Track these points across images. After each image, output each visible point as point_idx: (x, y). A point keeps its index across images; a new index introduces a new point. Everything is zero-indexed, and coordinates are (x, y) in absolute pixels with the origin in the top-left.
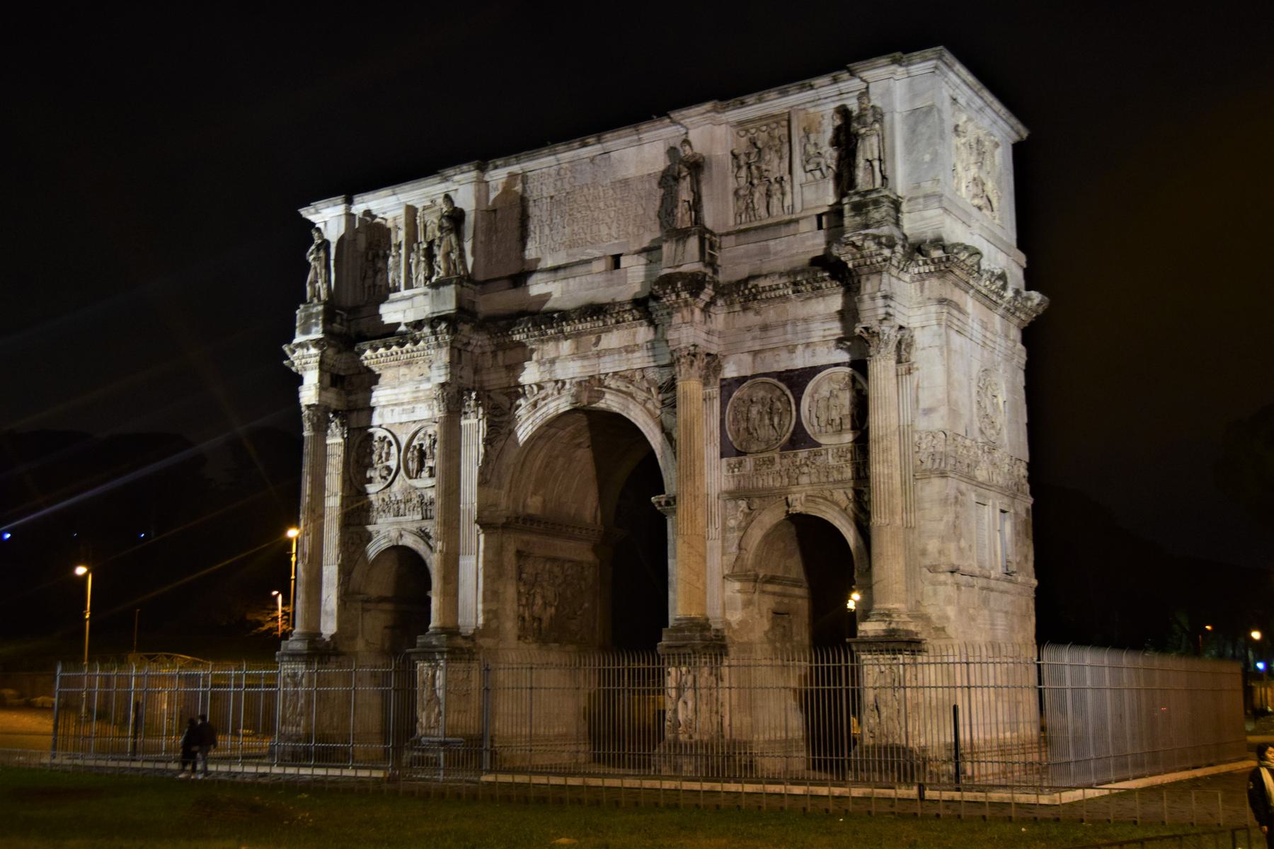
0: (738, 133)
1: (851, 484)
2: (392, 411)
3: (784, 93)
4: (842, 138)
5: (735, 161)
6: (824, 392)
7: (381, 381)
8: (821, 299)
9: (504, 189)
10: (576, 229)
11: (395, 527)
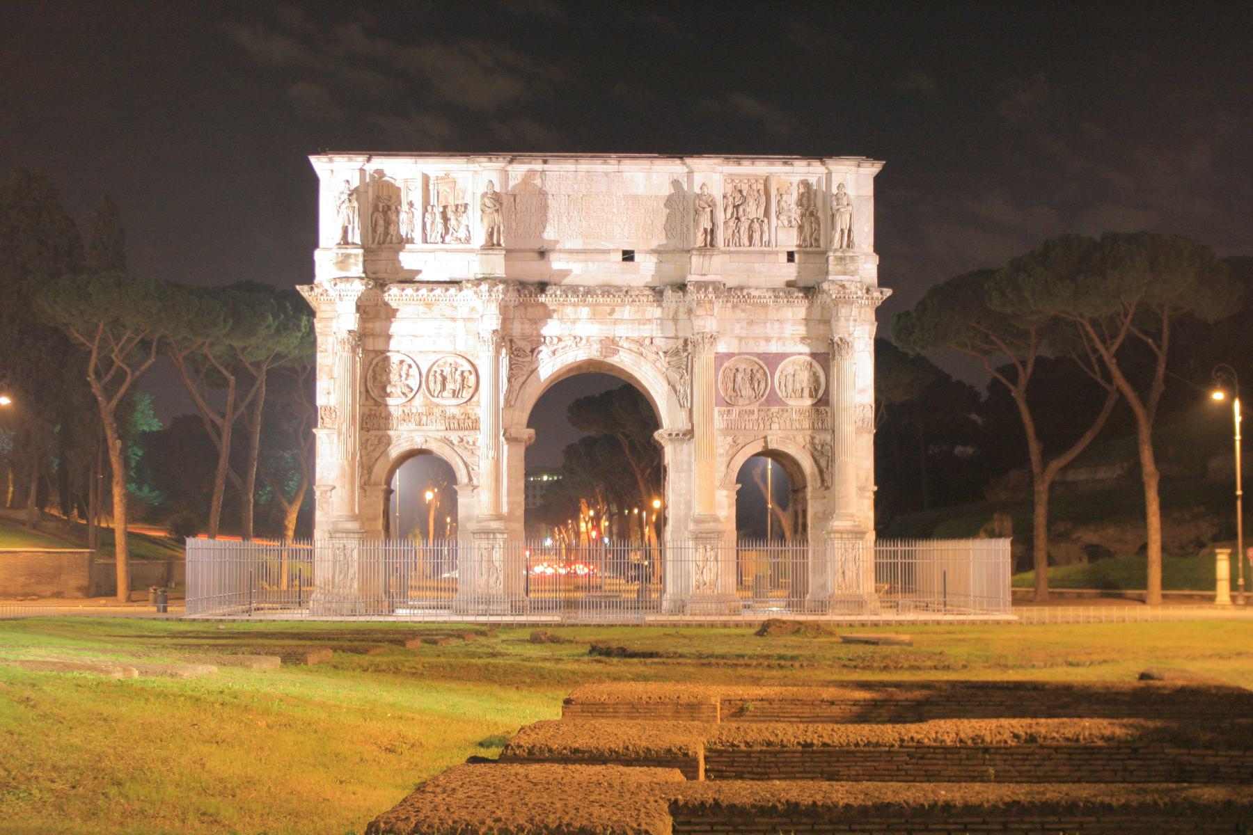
0: (725, 180)
1: (809, 432)
3: (772, 165)
4: (805, 201)
6: (790, 370)
7: (399, 315)
8: (790, 309)
9: (523, 180)
10: (592, 224)
11: (419, 434)
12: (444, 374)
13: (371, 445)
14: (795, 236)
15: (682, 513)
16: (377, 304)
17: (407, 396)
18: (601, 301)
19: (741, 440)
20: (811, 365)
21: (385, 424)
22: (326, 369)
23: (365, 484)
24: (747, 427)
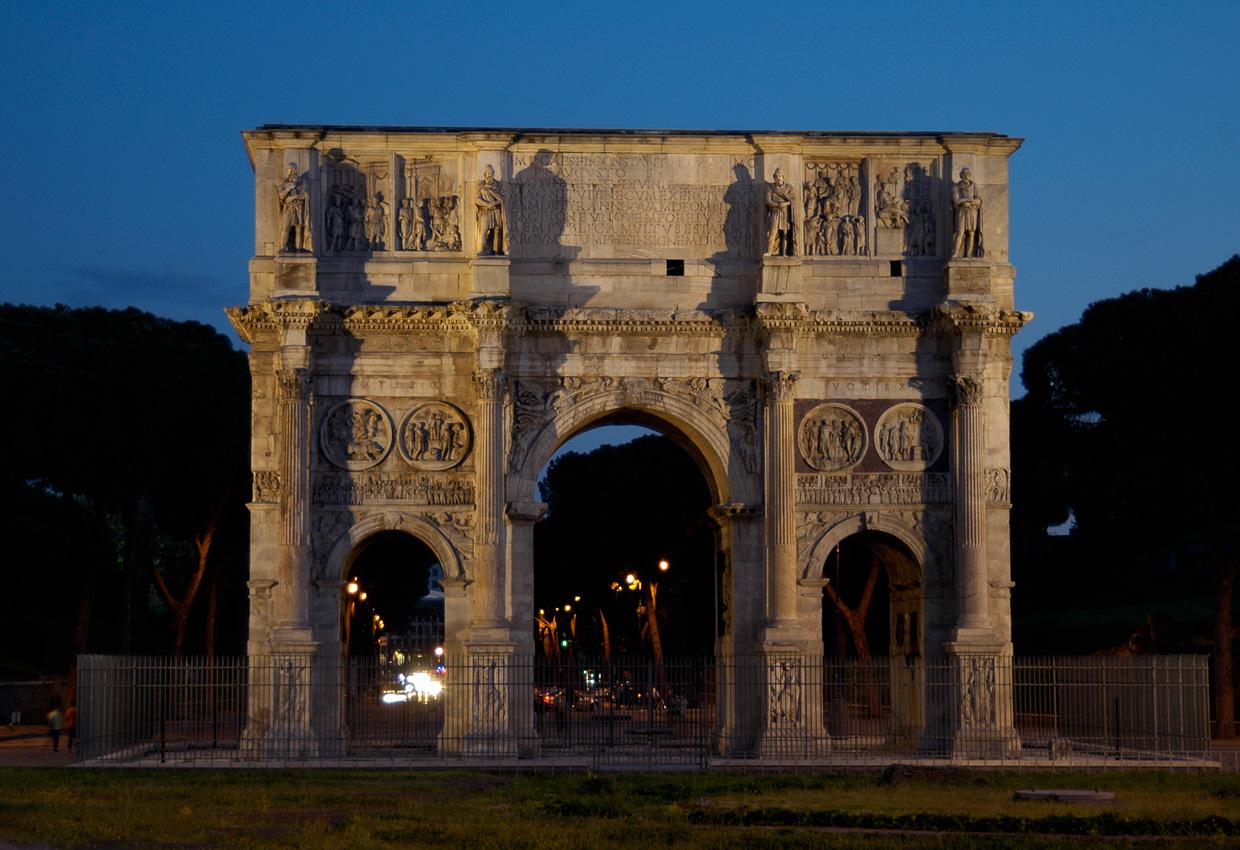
0: (806, 165)
2: (382, 383)
5: (806, 192)
7: (364, 348)
8: (895, 339)
9: (532, 164)
10: (626, 225)
11: (392, 510)
12: (426, 428)
13: (326, 525)
14: (901, 240)
15: (749, 618)
16: (334, 332)
17: (374, 459)
18: (639, 329)
19: (829, 518)
20: (923, 414)
21: (344, 495)
22: (265, 422)
23: (318, 579)
24: (837, 500)
